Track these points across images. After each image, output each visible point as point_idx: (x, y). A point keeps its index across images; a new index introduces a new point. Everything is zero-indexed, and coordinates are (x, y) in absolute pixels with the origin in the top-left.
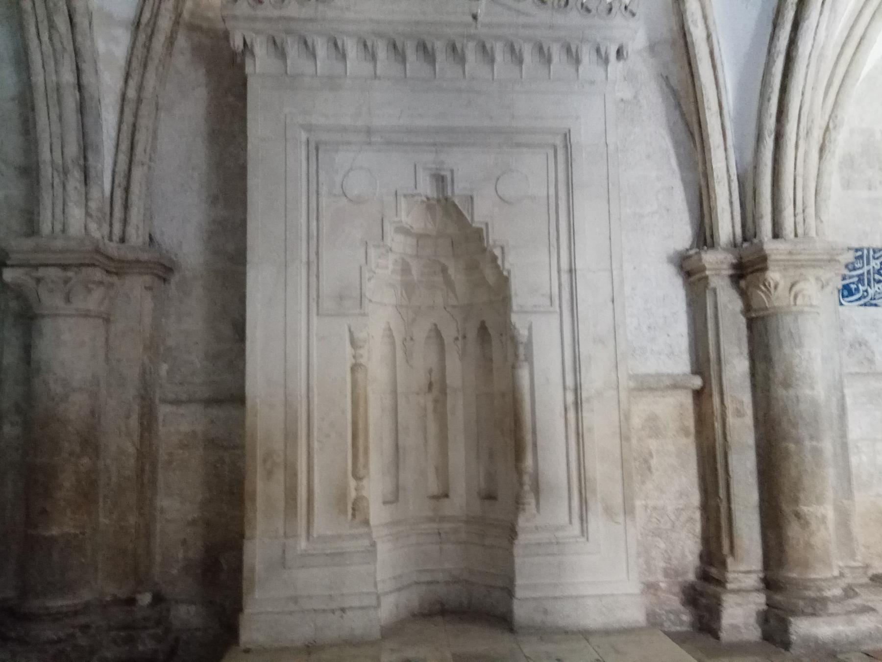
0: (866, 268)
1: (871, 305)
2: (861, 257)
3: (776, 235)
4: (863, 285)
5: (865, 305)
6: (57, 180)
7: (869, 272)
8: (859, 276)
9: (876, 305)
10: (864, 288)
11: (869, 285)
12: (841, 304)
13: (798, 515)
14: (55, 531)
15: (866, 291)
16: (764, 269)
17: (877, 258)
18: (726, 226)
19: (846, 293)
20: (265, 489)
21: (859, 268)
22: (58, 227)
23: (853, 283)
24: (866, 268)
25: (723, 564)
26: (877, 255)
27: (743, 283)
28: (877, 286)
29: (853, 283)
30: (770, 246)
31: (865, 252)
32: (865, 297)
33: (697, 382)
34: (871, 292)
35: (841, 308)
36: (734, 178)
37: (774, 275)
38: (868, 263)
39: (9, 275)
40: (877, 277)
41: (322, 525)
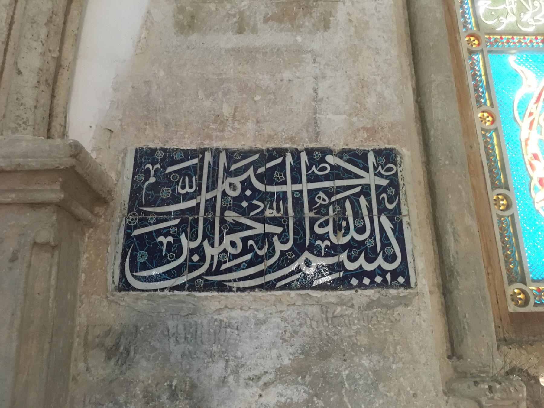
0: (205, 196)
1: (209, 286)
2: (197, 170)
4: (193, 238)
5: (191, 286)
7: (211, 204)
8: (183, 212)
9: (221, 287)
10: (194, 245)
11: (208, 236)
12: (125, 286)
15: (200, 250)
17: (237, 173)
19: (142, 257)
21: (187, 197)
23: (166, 232)
24: (205, 196)
26: (233, 167)
28: (227, 239)
29: (166, 232)
31: (208, 157)
32: (194, 267)
34: (209, 251)
35: (128, 297)
38: (212, 186)
40: (231, 216)
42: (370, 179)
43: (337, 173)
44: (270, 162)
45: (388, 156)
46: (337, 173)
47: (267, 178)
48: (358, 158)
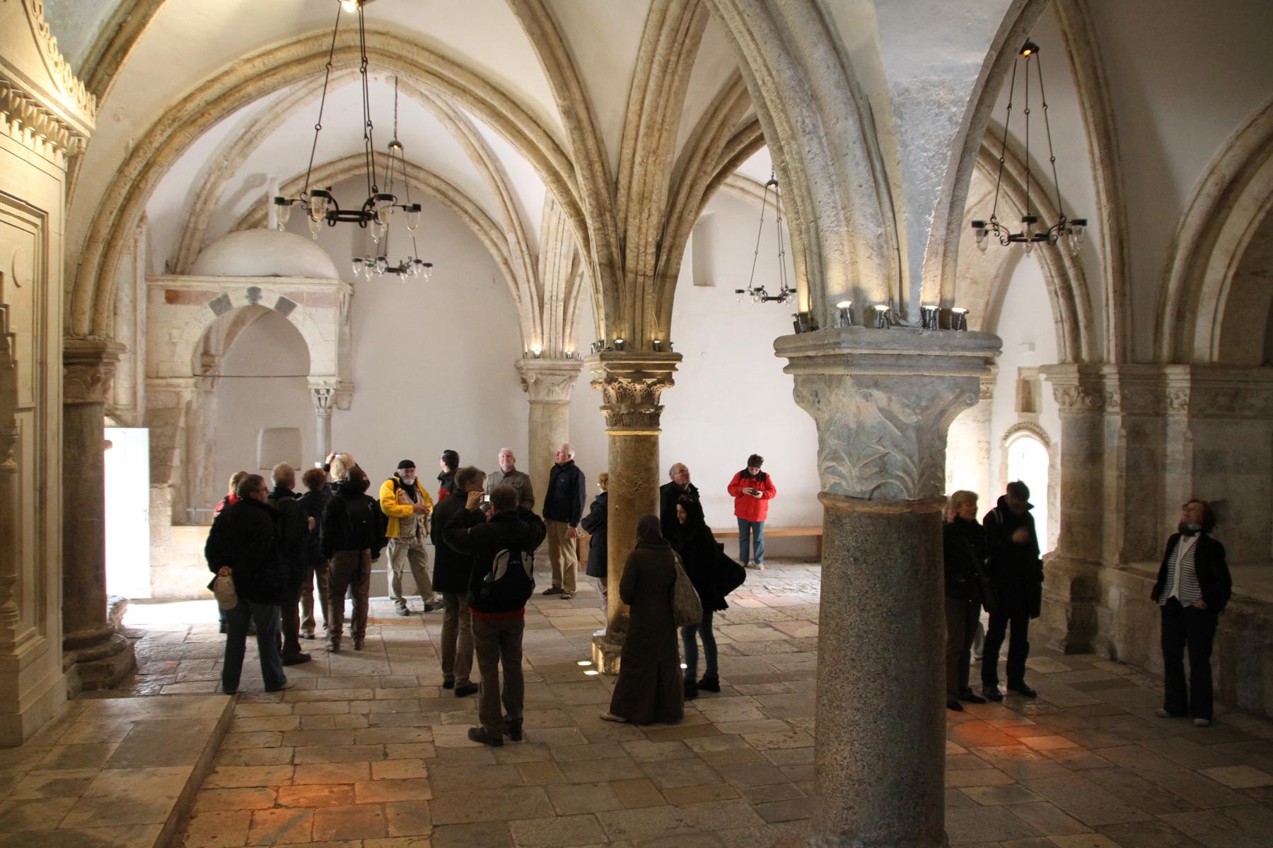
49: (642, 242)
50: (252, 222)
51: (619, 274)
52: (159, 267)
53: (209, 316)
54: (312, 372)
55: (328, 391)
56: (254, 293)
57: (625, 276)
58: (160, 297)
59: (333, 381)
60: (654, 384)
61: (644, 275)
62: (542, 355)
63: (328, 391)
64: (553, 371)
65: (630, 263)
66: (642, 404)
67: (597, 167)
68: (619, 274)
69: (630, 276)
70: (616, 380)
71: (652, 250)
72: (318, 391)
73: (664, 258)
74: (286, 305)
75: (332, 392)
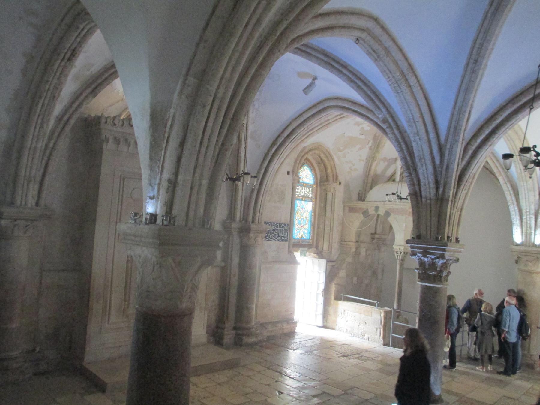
3: (253, 222)
6: (25, 184)
13: (247, 308)
14: (14, 326)
16: (249, 233)
18: (239, 215)
20: (96, 307)
22: (23, 203)
25: (224, 323)
27: (241, 234)
30: (253, 226)
33: (223, 264)
36: (243, 199)
37: (252, 235)
39: (3, 222)
41: (113, 319)
42: (286, 228)
43: (283, 227)
44: (277, 224)
45: (288, 225)
46: (283, 227)
47: (277, 227)
48: (285, 225)
49: (427, 183)
50: (392, 179)
51: (419, 199)
52: (355, 196)
53: (361, 217)
54: (395, 243)
55: (401, 253)
56: (377, 208)
57: (421, 199)
58: (347, 209)
59: (402, 248)
60: (435, 259)
61: (430, 199)
62: (522, 245)
63: (401, 253)
64: (527, 253)
65: (423, 194)
66: (429, 269)
67: (404, 146)
68: (419, 199)
69: (424, 200)
70: (415, 255)
71: (432, 186)
72: (397, 252)
73: (441, 190)
74: (388, 214)
75: (402, 253)
